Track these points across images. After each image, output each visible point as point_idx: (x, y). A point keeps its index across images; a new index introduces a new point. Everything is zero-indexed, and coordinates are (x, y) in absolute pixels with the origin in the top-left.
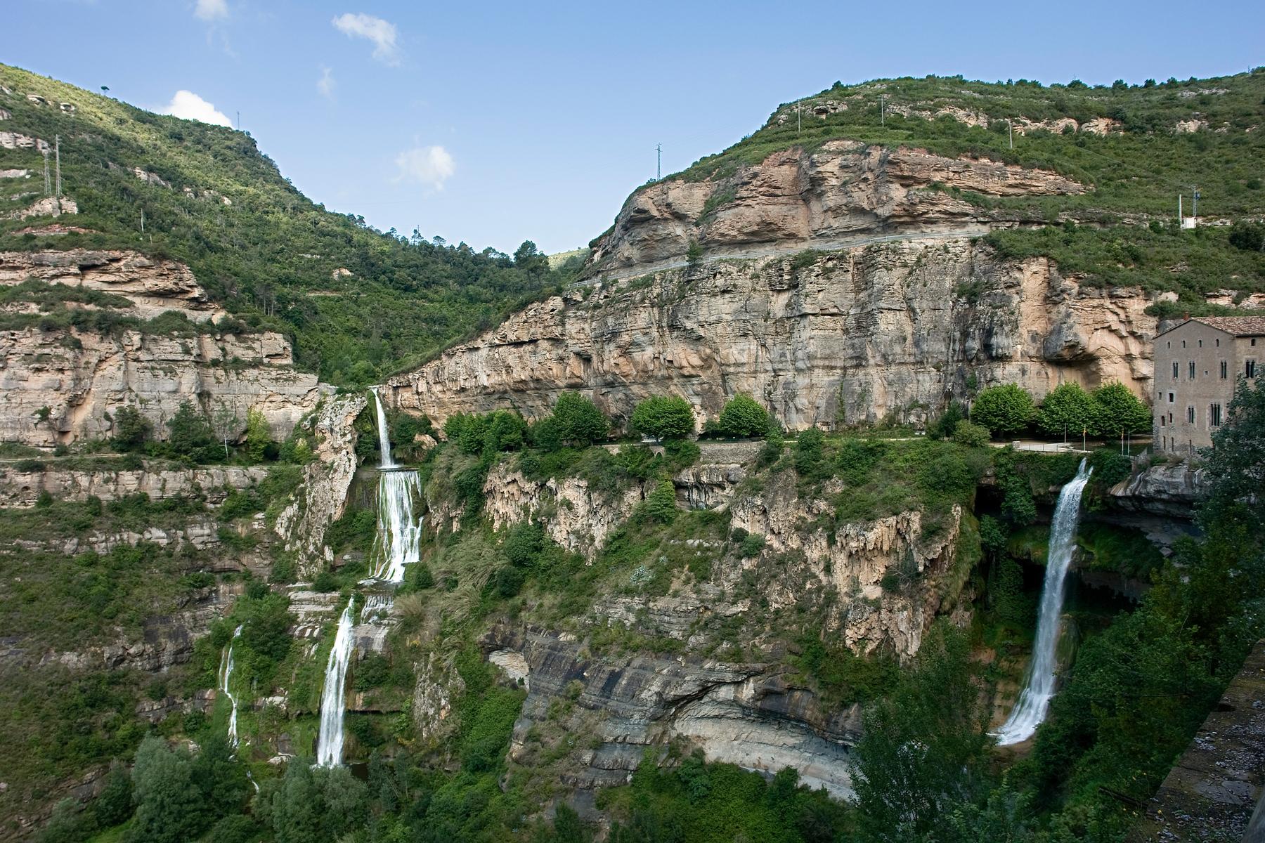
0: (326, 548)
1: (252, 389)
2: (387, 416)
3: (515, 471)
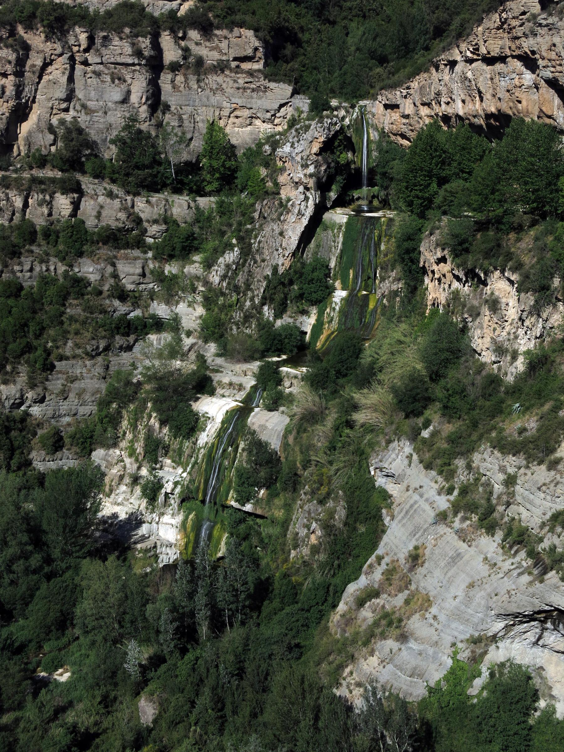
1: (215, 99)
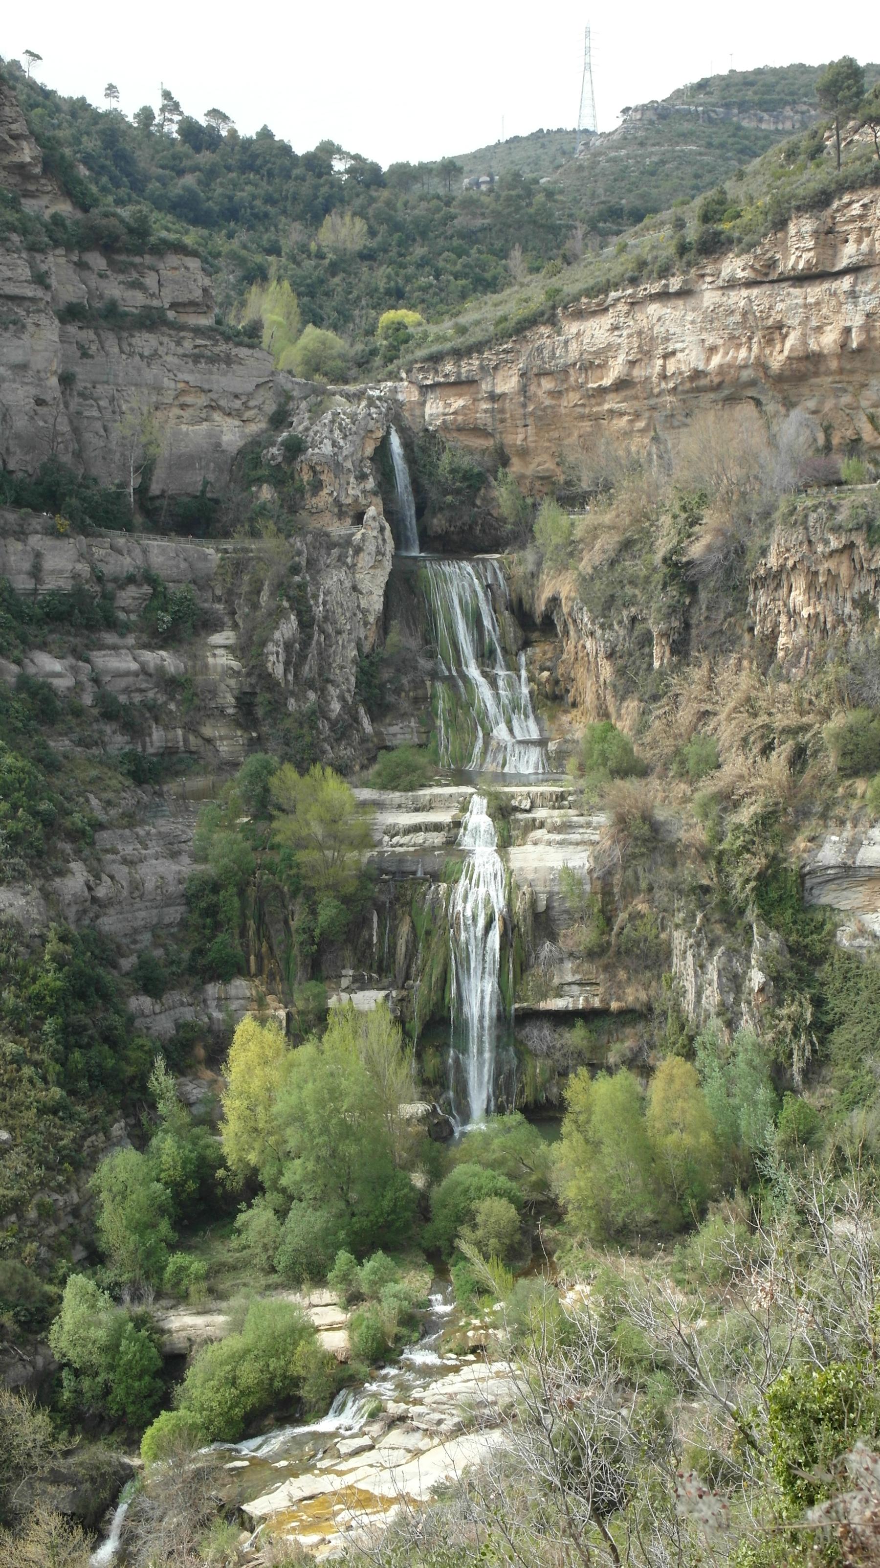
1: (150, 374)
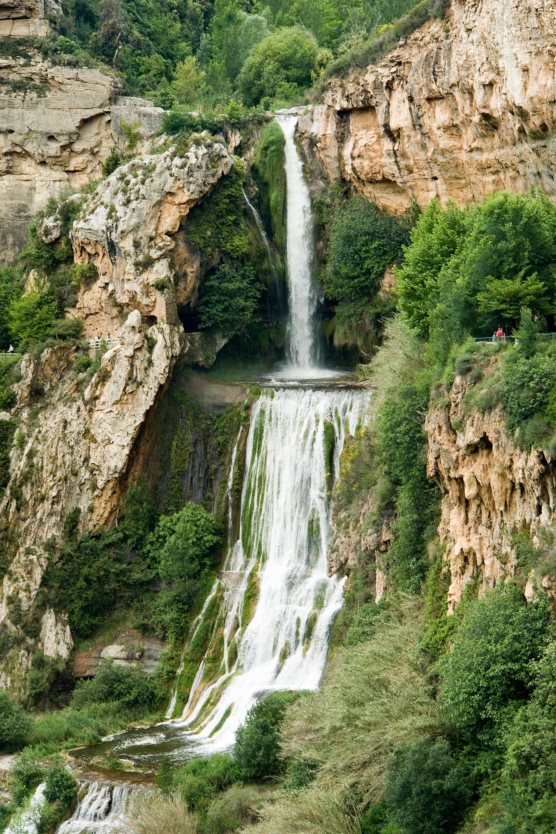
0: (49, 618)
2: (317, 207)
3: (487, 408)
